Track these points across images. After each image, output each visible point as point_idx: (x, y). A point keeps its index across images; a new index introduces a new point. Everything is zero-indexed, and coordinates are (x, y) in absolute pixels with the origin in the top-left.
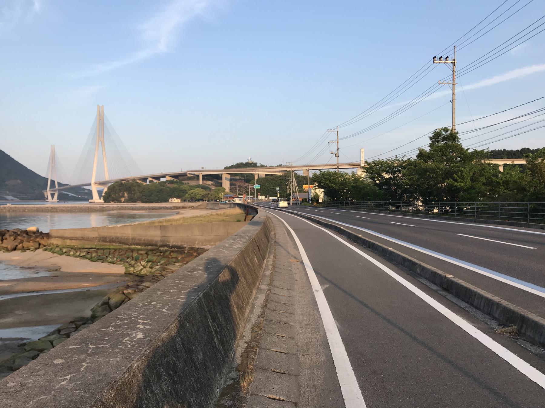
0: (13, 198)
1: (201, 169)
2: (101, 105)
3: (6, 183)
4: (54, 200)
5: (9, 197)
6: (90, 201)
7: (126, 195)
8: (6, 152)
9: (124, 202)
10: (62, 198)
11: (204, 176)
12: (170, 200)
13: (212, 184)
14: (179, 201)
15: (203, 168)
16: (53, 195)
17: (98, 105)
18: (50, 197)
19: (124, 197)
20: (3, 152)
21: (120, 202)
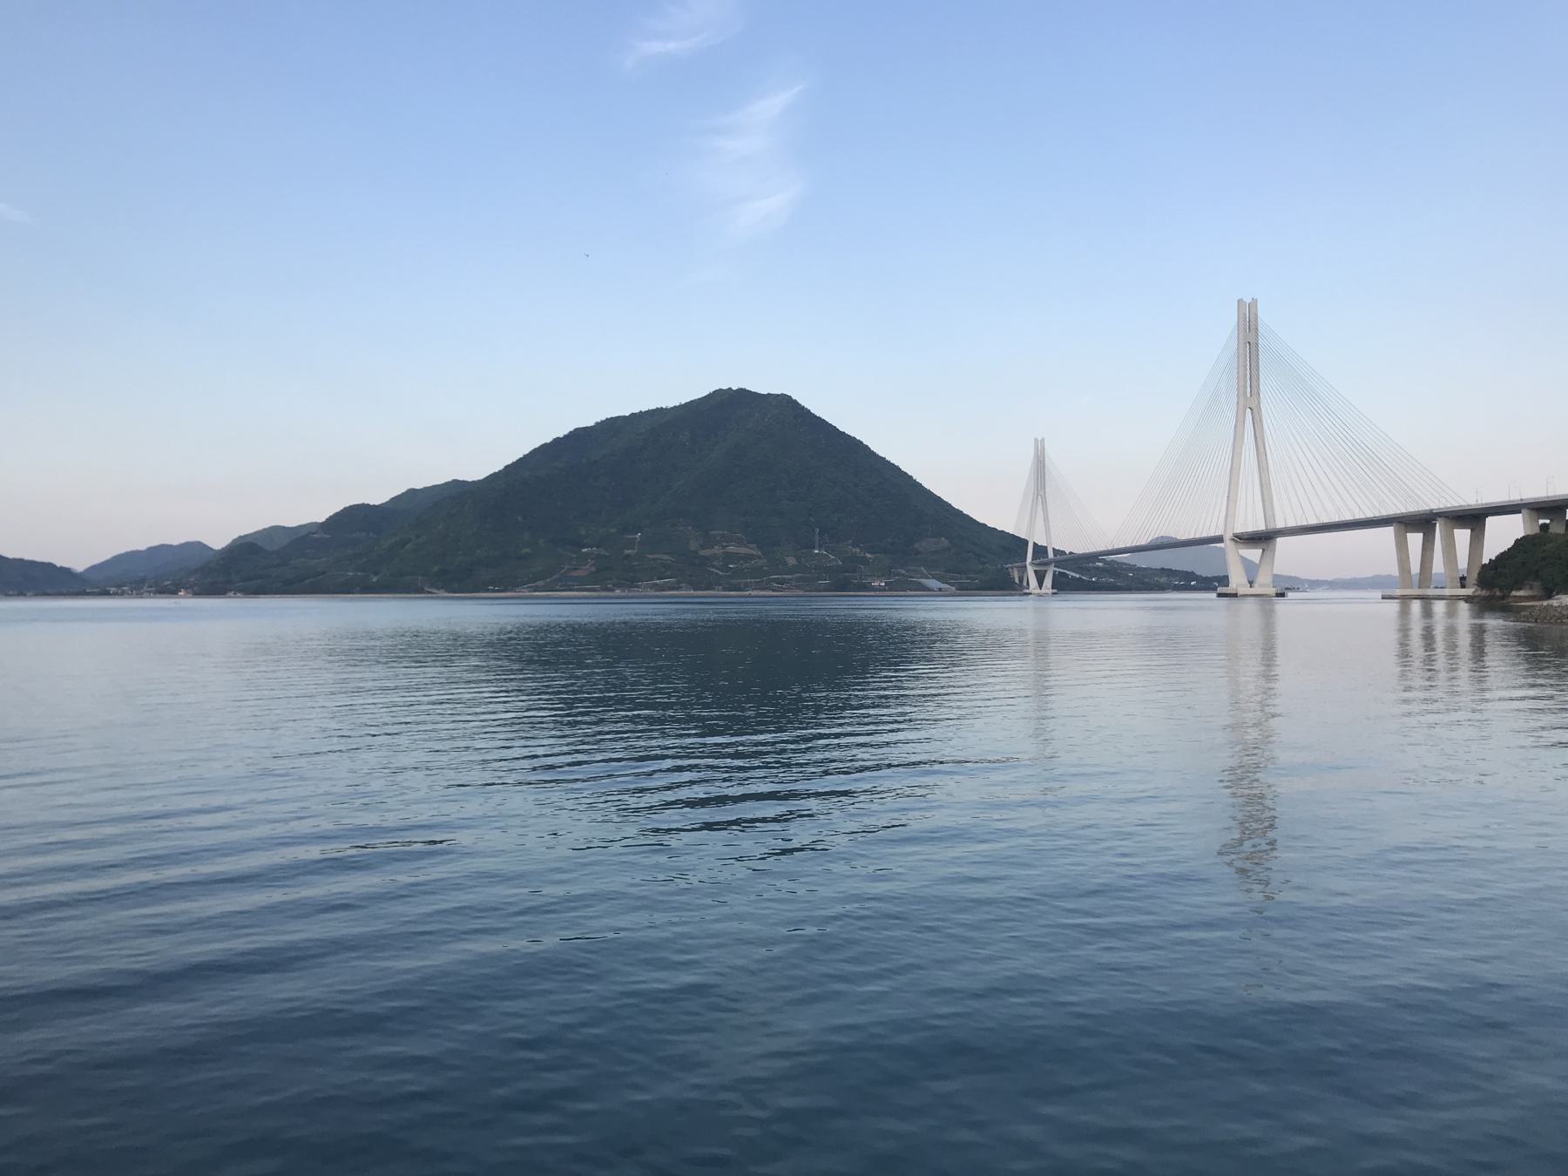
2: (1248, 300)
3: (916, 545)
5: (934, 583)
6: (1220, 590)
10: (1063, 585)
18: (1033, 582)
20: (898, 468)
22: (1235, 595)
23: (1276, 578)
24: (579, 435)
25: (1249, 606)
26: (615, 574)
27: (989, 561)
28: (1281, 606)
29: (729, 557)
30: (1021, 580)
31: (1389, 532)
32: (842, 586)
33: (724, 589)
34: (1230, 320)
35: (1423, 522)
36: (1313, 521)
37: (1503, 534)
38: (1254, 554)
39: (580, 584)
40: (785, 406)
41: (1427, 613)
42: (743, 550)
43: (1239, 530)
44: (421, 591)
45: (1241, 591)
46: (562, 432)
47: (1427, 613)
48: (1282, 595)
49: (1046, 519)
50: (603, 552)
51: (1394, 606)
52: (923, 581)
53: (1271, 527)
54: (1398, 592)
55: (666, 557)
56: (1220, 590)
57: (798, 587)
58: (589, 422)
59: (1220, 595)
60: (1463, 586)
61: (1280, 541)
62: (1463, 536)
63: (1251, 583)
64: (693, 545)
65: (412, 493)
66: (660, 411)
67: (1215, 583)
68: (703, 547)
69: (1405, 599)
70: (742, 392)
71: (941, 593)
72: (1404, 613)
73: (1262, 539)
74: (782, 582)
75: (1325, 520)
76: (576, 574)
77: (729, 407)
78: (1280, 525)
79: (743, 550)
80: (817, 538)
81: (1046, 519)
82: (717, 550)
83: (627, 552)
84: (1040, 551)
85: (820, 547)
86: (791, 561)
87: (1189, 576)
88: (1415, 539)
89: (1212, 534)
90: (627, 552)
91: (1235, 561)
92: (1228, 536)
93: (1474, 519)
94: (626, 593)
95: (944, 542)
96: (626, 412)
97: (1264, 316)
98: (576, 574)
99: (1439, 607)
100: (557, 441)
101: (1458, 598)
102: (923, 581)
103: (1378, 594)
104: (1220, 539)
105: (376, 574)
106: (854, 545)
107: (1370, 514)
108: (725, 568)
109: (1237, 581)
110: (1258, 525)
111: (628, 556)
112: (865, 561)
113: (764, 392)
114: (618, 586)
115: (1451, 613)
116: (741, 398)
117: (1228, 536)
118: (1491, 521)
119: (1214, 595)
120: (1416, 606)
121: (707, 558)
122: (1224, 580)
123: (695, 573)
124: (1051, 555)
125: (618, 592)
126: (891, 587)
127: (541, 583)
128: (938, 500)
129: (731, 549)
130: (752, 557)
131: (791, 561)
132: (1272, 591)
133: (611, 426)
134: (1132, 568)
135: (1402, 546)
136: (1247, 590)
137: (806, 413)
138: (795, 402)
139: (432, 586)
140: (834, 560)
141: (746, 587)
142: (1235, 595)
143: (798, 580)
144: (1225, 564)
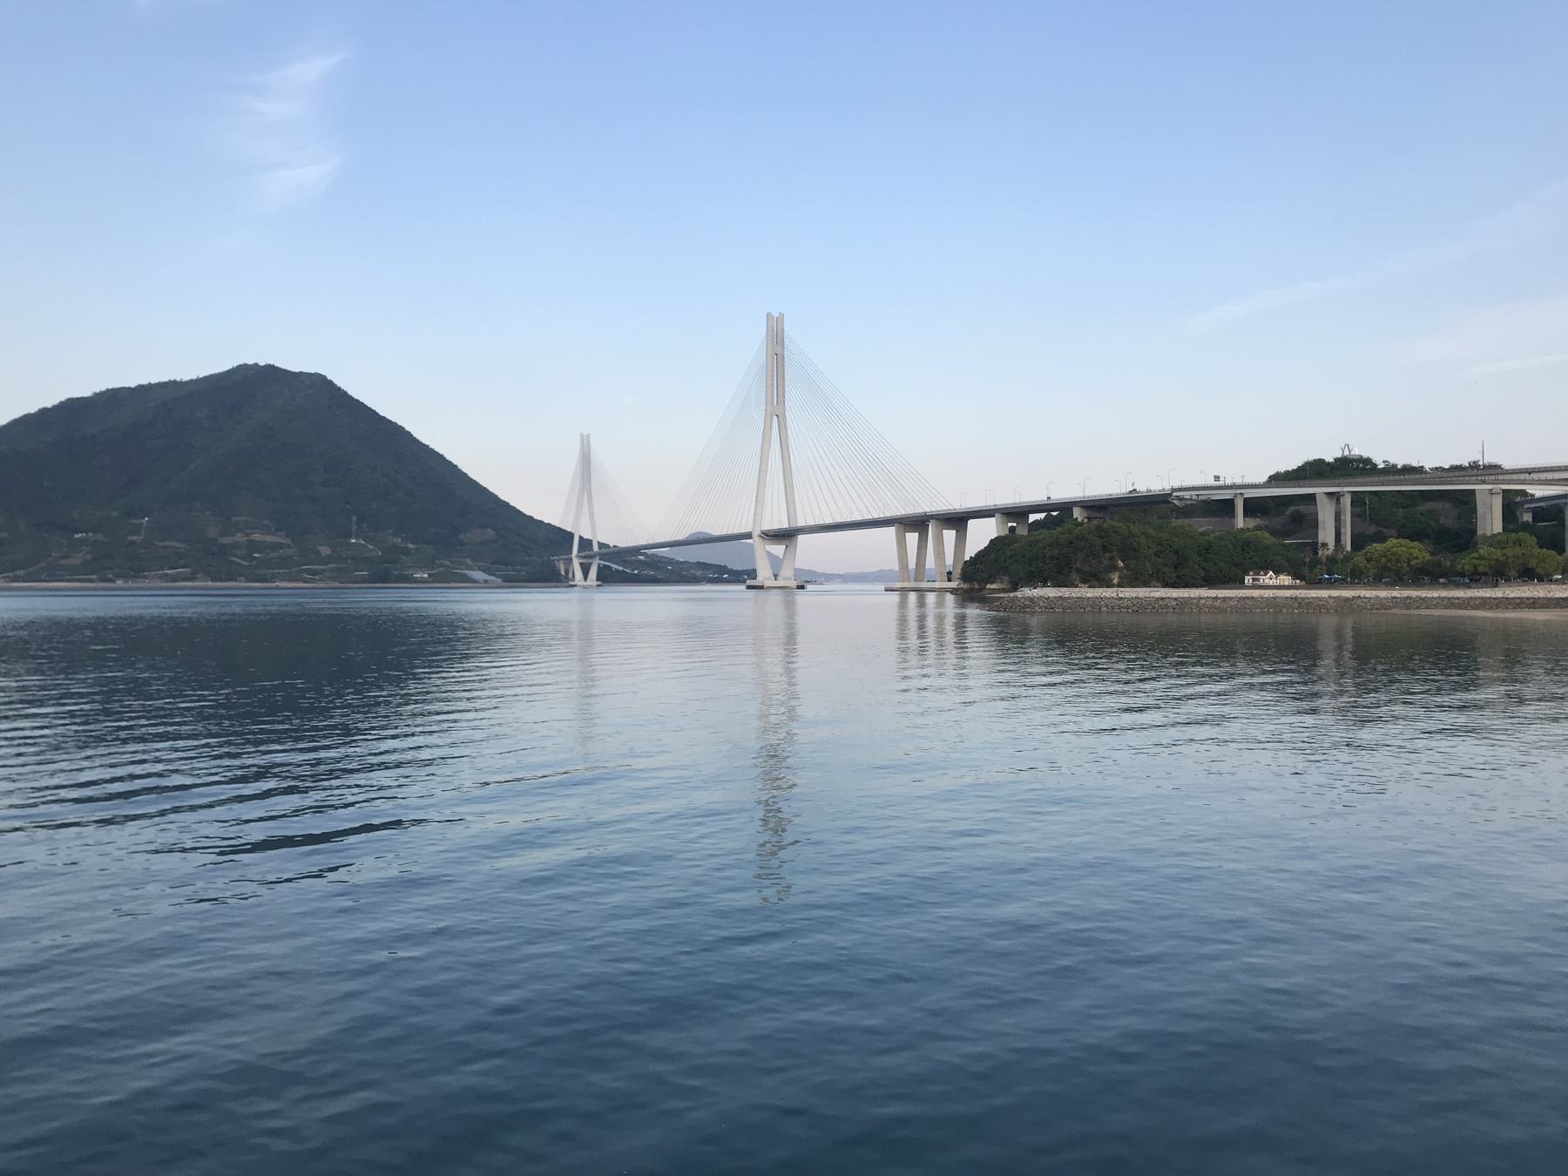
0: (485, 576)
1: (1212, 482)
4: (589, 583)
5: (479, 575)
6: (749, 582)
7: (1121, 564)
8: (448, 458)
9: (1119, 585)
10: (606, 577)
11: (1248, 503)
12: (1248, 580)
13: (1258, 528)
14: (1285, 579)
15: (1217, 478)
16: (586, 571)
17: (769, 315)
18: (579, 574)
19: (1114, 568)
21: (1109, 585)
22: (762, 587)
23: (798, 572)
24: (72, 409)
25: (775, 598)
26: (117, 562)
28: (801, 597)
29: (253, 546)
30: (567, 572)
32: (383, 575)
34: (760, 333)
35: (918, 523)
36: (829, 521)
37: (981, 534)
38: (778, 549)
39: (72, 573)
40: (319, 384)
41: (921, 604)
42: (269, 538)
43: (766, 527)
45: (767, 584)
47: (921, 604)
48: (802, 587)
49: (591, 513)
50: (100, 537)
51: (894, 598)
53: (793, 525)
54: (898, 585)
55: (177, 545)
56: (749, 582)
57: (333, 579)
58: (87, 392)
59: (749, 587)
61: (801, 538)
62: (950, 535)
63: (776, 576)
64: (212, 532)
66: (173, 384)
67: (743, 576)
68: (224, 534)
69: (904, 591)
70: (271, 370)
71: (486, 585)
72: (903, 604)
73: (785, 536)
74: (315, 573)
75: (840, 520)
76: (64, 562)
77: (253, 386)
78: (801, 523)
79: (269, 538)
80: (354, 527)
81: (591, 513)
82: (239, 537)
84: (585, 544)
85: (357, 537)
86: (325, 551)
87: (722, 569)
88: (912, 538)
89: (743, 530)
91: (763, 556)
92: (756, 534)
93: (957, 521)
94: (130, 584)
95: (490, 533)
96: (132, 382)
99: (931, 598)
100: (44, 412)
101: (946, 590)
103: (882, 587)
104: (749, 536)
106: (395, 535)
107: (876, 515)
108: (250, 557)
109: (764, 575)
110: (786, 526)
111: (133, 543)
112: (406, 552)
113: (295, 369)
114: (119, 576)
115: (940, 604)
116: (271, 374)
117: (756, 534)
119: (743, 587)
120: (912, 597)
121: (225, 546)
122: (752, 574)
123: (214, 563)
124: (596, 548)
125: (119, 583)
126: (434, 579)
127: (21, 572)
128: (484, 491)
129: (257, 537)
130: (281, 546)
131: (325, 551)
132: (793, 584)
134: (671, 562)
135: (902, 544)
136: (771, 583)
137: (343, 395)
138: (331, 382)
140: (374, 551)
141: (273, 578)
142: (762, 587)
144: (753, 559)
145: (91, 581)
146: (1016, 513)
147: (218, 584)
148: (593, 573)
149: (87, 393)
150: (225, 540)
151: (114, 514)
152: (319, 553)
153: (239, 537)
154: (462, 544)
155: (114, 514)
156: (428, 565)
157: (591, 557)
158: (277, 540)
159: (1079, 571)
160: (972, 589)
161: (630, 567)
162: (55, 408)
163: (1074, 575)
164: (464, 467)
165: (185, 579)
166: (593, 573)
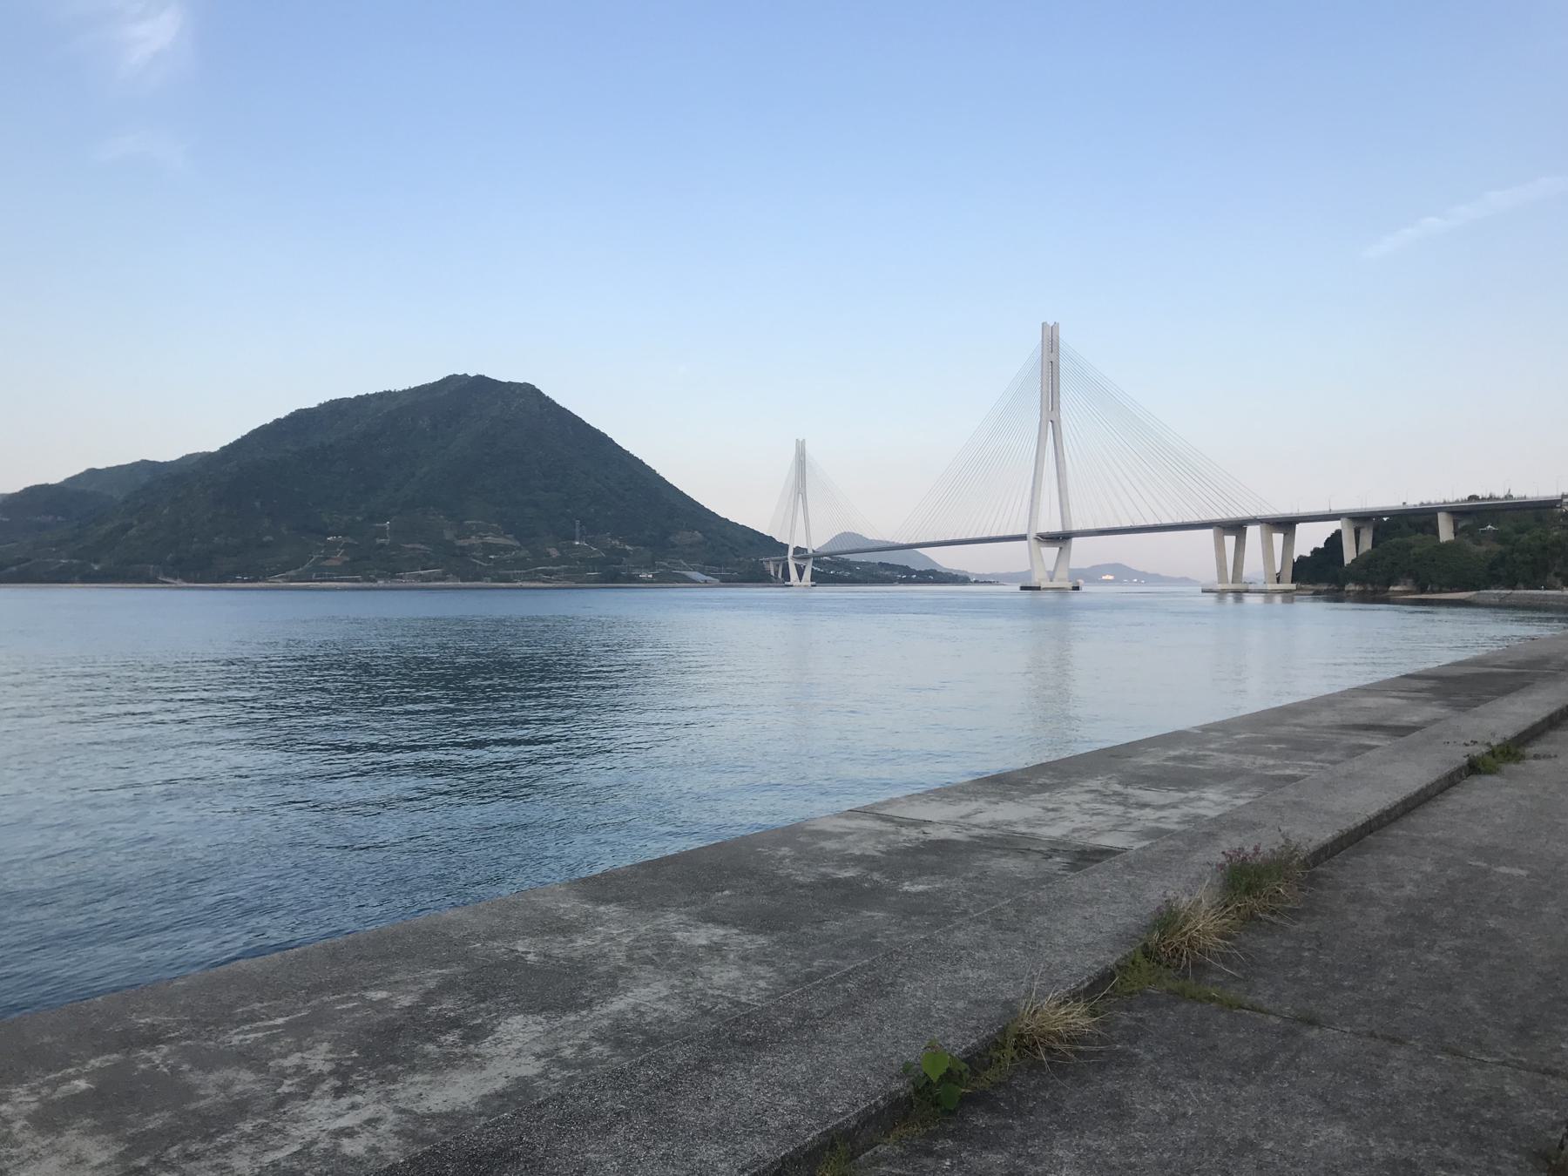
3: (672, 538)
10: (818, 579)
22: (1039, 588)
23: (1075, 574)
24: (301, 420)
26: (371, 564)
27: (742, 558)
28: (1075, 597)
29: (489, 548)
31: (1209, 533)
33: (494, 581)
34: (1035, 340)
35: (1237, 528)
36: (1127, 524)
37: (1309, 539)
38: (1051, 552)
40: (528, 394)
42: (501, 541)
44: (155, 581)
46: (282, 413)
48: (1077, 588)
50: (350, 541)
51: (1211, 598)
52: (689, 574)
54: (1220, 587)
57: (568, 579)
58: (312, 403)
59: (1023, 588)
60: (1278, 581)
62: (1278, 538)
64: (448, 535)
65: (92, 473)
68: (458, 537)
69: (1222, 593)
70: (481, 380)
73: (1060, 539)
74: (550, 573)
76: (327, 563)
77: (465, 399)
78: (1076, 526)
79: (501, 541)
82: (474, 540)
83: (379, 541)
84: (798, 550)
86: (554, 553)
87: (906, 570)
88: (1230, 541)
90: (379, 541)
93: (1286, 525)
97: (1065, 337)
98: (327, 563)
100: (278, 422)
102: (689, 574)
104: (1023, 538)
105: (96, 562)
106: (613, 537)
107: (1194, 518)
108: (485, 558)
110: (1056, 528)
111: (382, 545)
114: (380, 576)
116: (482, 384)
117: (1033, 535)
118: (1299, 527)
120: (1230, 598)
121: (461, 548)
123: (462, 567)
125: (381, 583)
127: (292, 573)
129: (490, 539)
130: (507, 549)
131: (554, 553)
132: (1069, 585)
133: (336, 409)
135: (1220, 547)
139: (166, 575)
143: (566, 571)
145: (356, 581)
146: (1360, 520)
147: (468, 584)
148: (807, 574)
149: (314, 405)
150: (460, 543)
151: (359, 518)
152: (548, 555)
153: (474, 540)
154: (674, 546)
155: (359, 518)
156: (650, 566)
157: (806, 558)
158: (509, 542)
159: (1557, 575)
160: (1363, 592)
161: (841, 568)
162: (288, 418)
163: (1551, 578)
164: (661, 471)
165: (436, 580)
166: (807, 574)
